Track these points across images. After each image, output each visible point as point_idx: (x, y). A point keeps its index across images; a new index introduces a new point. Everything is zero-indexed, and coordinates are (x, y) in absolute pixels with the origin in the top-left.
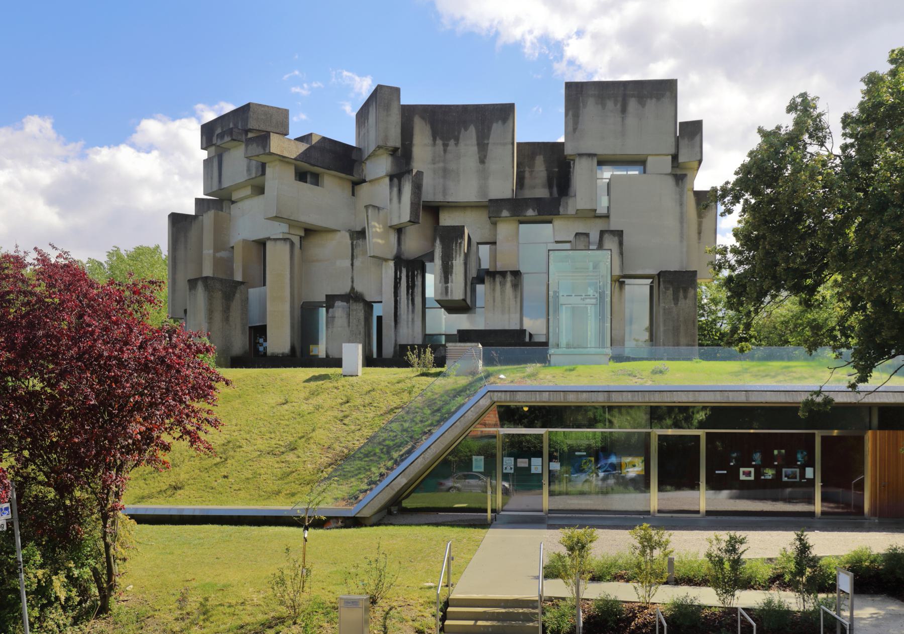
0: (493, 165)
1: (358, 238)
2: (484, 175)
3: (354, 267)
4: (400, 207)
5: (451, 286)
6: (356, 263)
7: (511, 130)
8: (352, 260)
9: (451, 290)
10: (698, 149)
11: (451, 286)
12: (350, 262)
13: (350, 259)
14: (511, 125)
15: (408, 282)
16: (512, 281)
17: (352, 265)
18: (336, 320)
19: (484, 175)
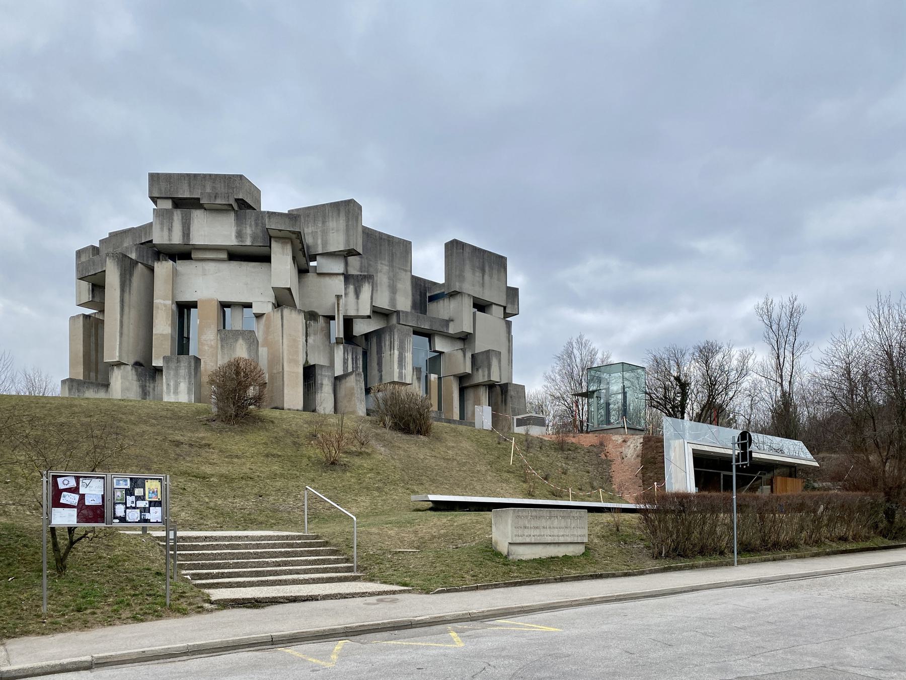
0: (400, 286)
1: (310, 320)
2: (393, 290)
3: (308, 343)
4: (357, 302)
5: (405, 373)
6: (310, 340)
7: (410, 262)
8: (306, 337)
9: (405, 376)
10: (516, 306)
11: (405, 373)
12: (305, 339)
13: (305, 336)
14: (410, 257)
15: (353, 363)
16: (417, 375)
17: (306, 341)
18: (324, 386)
19: (393, 290)
